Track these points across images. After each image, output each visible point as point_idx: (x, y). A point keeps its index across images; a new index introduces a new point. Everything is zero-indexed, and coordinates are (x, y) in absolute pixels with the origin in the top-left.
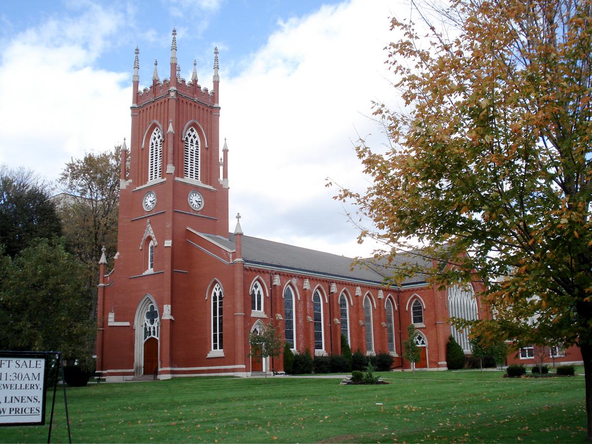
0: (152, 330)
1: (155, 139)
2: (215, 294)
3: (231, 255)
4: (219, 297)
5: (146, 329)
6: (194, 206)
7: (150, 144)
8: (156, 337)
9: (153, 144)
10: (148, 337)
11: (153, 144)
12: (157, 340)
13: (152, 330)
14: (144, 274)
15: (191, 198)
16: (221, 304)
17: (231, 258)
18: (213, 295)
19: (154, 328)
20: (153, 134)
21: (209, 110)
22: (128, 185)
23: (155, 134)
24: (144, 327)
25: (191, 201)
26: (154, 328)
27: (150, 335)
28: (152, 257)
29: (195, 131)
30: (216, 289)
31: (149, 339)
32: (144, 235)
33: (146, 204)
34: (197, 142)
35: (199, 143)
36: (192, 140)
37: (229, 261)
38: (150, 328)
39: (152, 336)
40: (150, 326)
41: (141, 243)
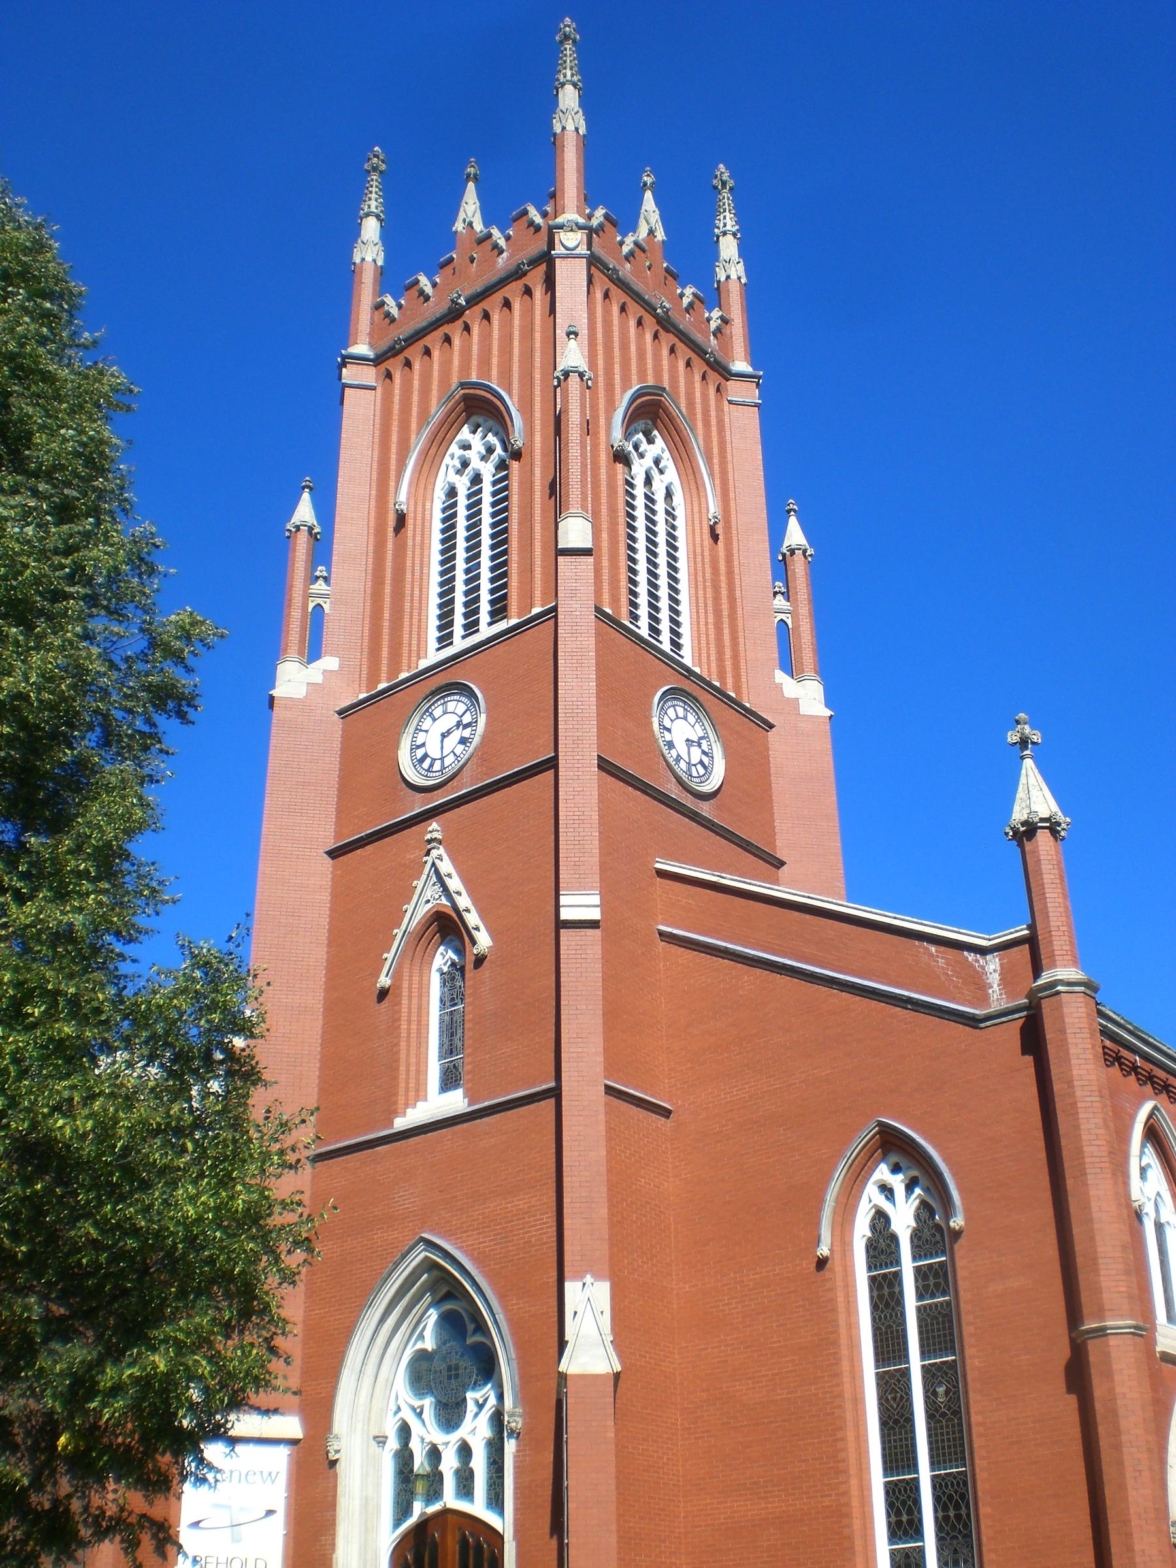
0: (449, 1464)
1: (465, 464)
2: (881, 1219)
3: (992, 965)
4: (916, 1236)
5: (404, 1457)
6: (683, 765)
7: (439, 496)
8: (478, 1507)
9: (452, 492)
10: (419, 1509)
11: (452, 492)
12: (497, 1537)
13: (449, 1464)
14: (400, 1124)
15: (667, 723)
16: (929, 1280)
17: (994, 979)
18: (862, 1229)
19: (465, 1451)
20: (454, 448)
21: (713, 377)
22: (319, 679)
23: (466, 447)
24: (393, 1444)
25: (668, 737)
26: (465, 1451)
27: (435, 1492)
28: (450, 1029)
29: (659, 441)
30: (886, 1190)
31: (424, 1525)
32: (410, 908)
33: (420, 753)
34: (669, 495)
35: (678, 499)
36: (648, 481)
37: (984, 999)
38: (434, 1454)
39: (450, 1499)
40: (437, 1436)
41: (389, 956)
